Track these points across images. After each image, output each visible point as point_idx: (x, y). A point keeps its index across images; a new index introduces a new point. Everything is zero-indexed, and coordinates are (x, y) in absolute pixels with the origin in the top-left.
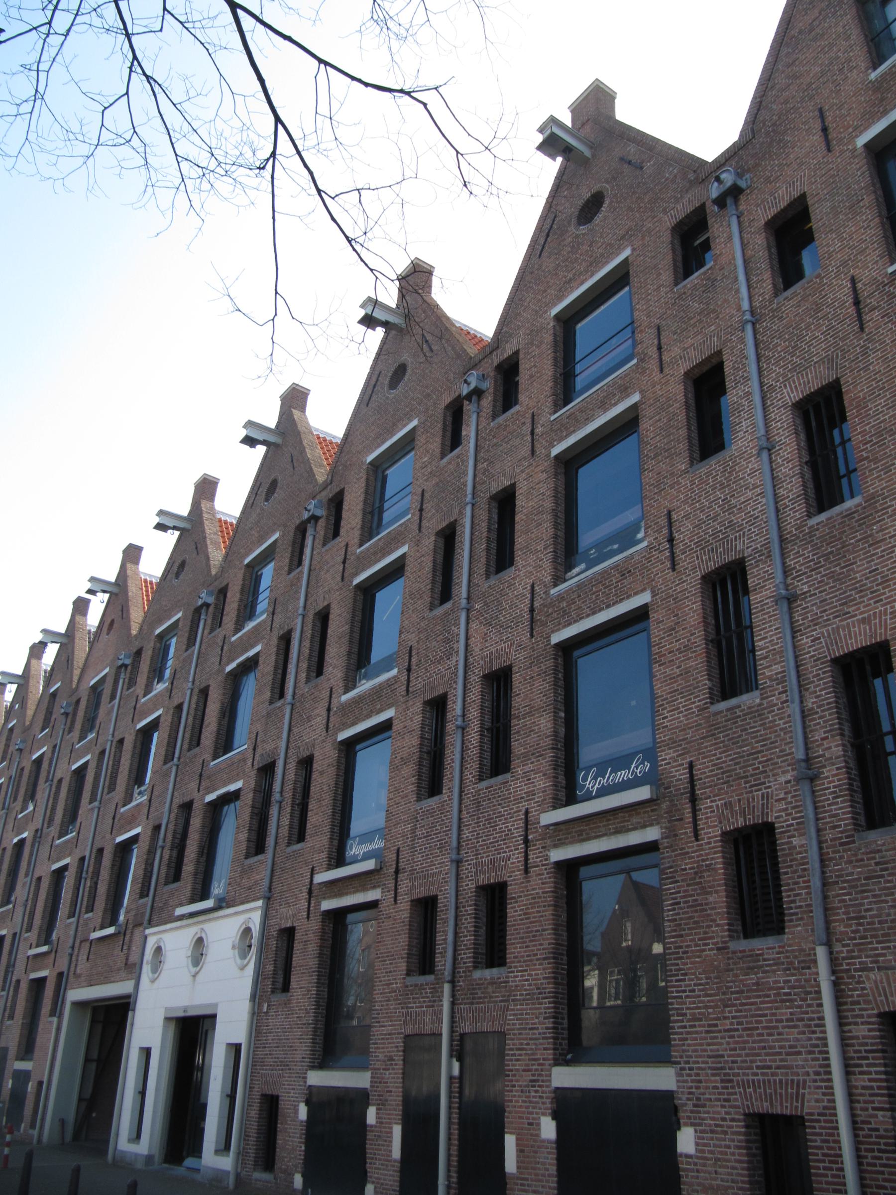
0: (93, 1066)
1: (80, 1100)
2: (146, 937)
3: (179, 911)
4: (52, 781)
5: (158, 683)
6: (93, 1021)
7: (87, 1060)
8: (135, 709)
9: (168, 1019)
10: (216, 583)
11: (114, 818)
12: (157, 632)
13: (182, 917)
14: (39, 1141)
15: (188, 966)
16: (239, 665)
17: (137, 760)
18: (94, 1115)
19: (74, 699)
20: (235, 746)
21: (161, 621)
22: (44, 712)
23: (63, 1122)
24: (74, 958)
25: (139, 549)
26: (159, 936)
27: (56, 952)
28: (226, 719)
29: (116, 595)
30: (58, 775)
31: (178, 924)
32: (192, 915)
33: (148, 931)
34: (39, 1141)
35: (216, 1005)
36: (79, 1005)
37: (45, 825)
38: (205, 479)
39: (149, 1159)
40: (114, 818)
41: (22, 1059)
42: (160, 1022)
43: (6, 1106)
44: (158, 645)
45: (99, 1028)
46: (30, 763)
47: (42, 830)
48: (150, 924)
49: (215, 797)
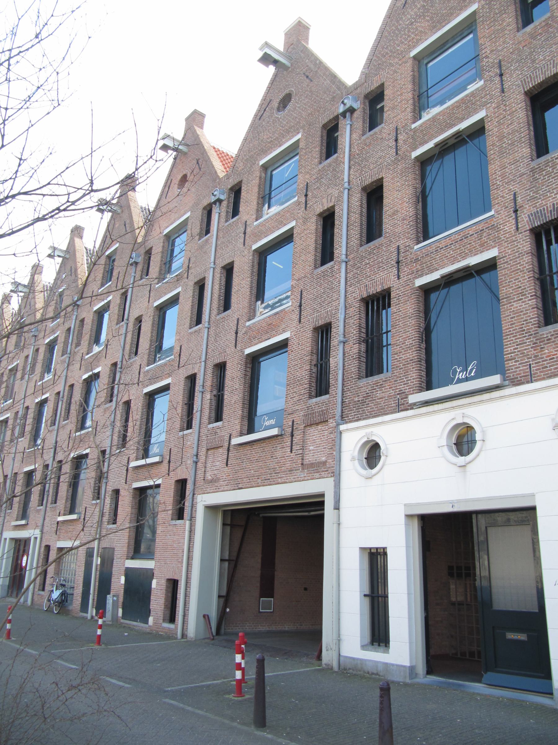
0: (226, 564)
1: (220, 597)
2: (341, 433)
3: (413, 398)
4: (128, 320)
5: (269, 207)
6: (224, 524)
7: (222, 560)
8: (245, 233)
9: (409, 517)
10: (359, 91)
11: (237, 333)
12: (262, 162)
13: (412, 406)
14: (184, 635)
15: (444, 457)
16: (437, 145)
17: (256, 278)
18: (228, 610)
19: (142, 251)
20: (431, 234)
21: (265, 152)
22: (102, 272)
23: (206, 617)
24: (200, 465)
25: (203, 116)
26: (368, 430)
27: (169, 462)
28: (420, 204)
29: (185, 154)
30: (135, 314)
31: (410, 413)
32: (427, 403)
33: (342, 427)
34: (184, 635)
35: (533, 495)
36: (212, 509)
37: (127, 357)
38: (299, 22)
39: (412, 669)
40: (237, 333)
41: (132, 558)
42: (402, 519)
43: (121, 599)
44: (263, 175)
45: (228, 529)
46: (92, 313)
47: (122, 362)
48: (344, 419)
49: (439, 277)
